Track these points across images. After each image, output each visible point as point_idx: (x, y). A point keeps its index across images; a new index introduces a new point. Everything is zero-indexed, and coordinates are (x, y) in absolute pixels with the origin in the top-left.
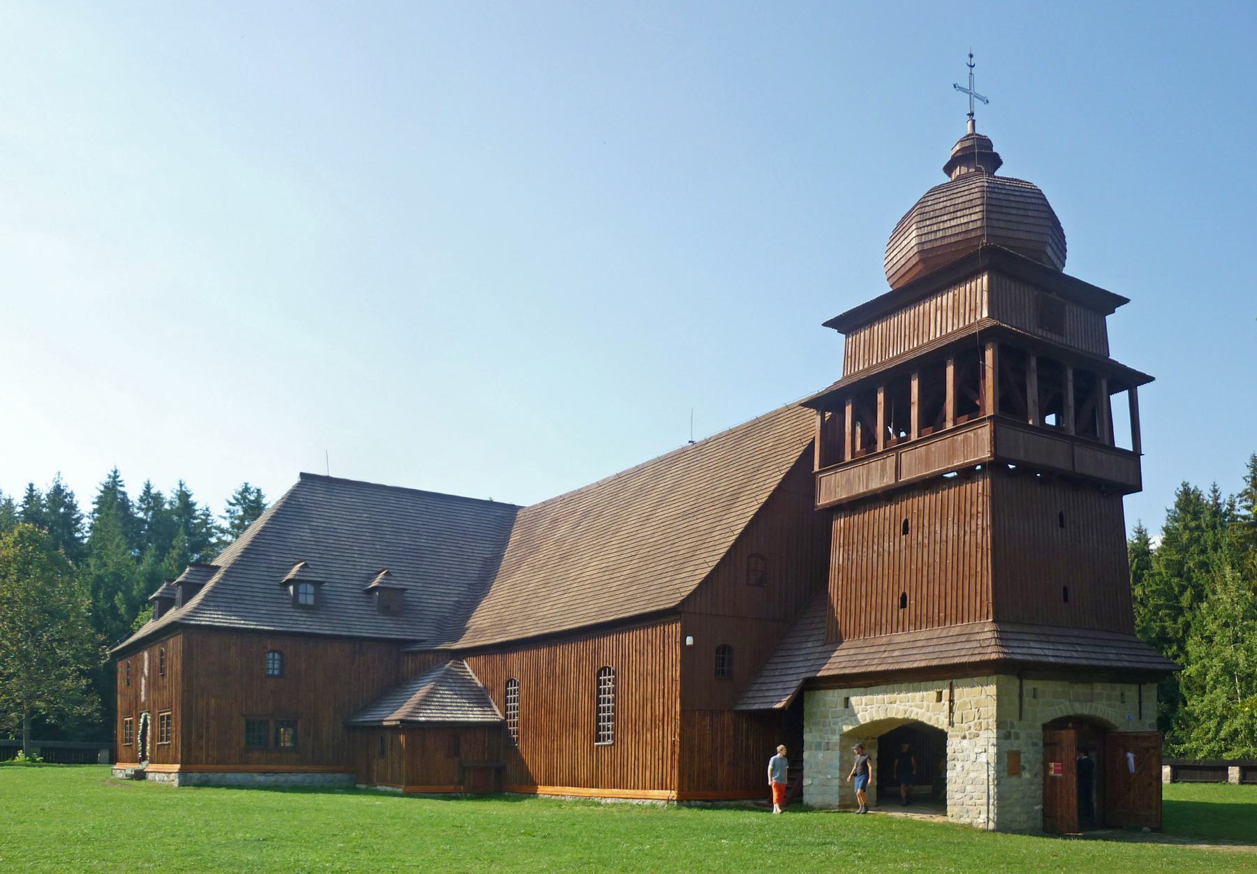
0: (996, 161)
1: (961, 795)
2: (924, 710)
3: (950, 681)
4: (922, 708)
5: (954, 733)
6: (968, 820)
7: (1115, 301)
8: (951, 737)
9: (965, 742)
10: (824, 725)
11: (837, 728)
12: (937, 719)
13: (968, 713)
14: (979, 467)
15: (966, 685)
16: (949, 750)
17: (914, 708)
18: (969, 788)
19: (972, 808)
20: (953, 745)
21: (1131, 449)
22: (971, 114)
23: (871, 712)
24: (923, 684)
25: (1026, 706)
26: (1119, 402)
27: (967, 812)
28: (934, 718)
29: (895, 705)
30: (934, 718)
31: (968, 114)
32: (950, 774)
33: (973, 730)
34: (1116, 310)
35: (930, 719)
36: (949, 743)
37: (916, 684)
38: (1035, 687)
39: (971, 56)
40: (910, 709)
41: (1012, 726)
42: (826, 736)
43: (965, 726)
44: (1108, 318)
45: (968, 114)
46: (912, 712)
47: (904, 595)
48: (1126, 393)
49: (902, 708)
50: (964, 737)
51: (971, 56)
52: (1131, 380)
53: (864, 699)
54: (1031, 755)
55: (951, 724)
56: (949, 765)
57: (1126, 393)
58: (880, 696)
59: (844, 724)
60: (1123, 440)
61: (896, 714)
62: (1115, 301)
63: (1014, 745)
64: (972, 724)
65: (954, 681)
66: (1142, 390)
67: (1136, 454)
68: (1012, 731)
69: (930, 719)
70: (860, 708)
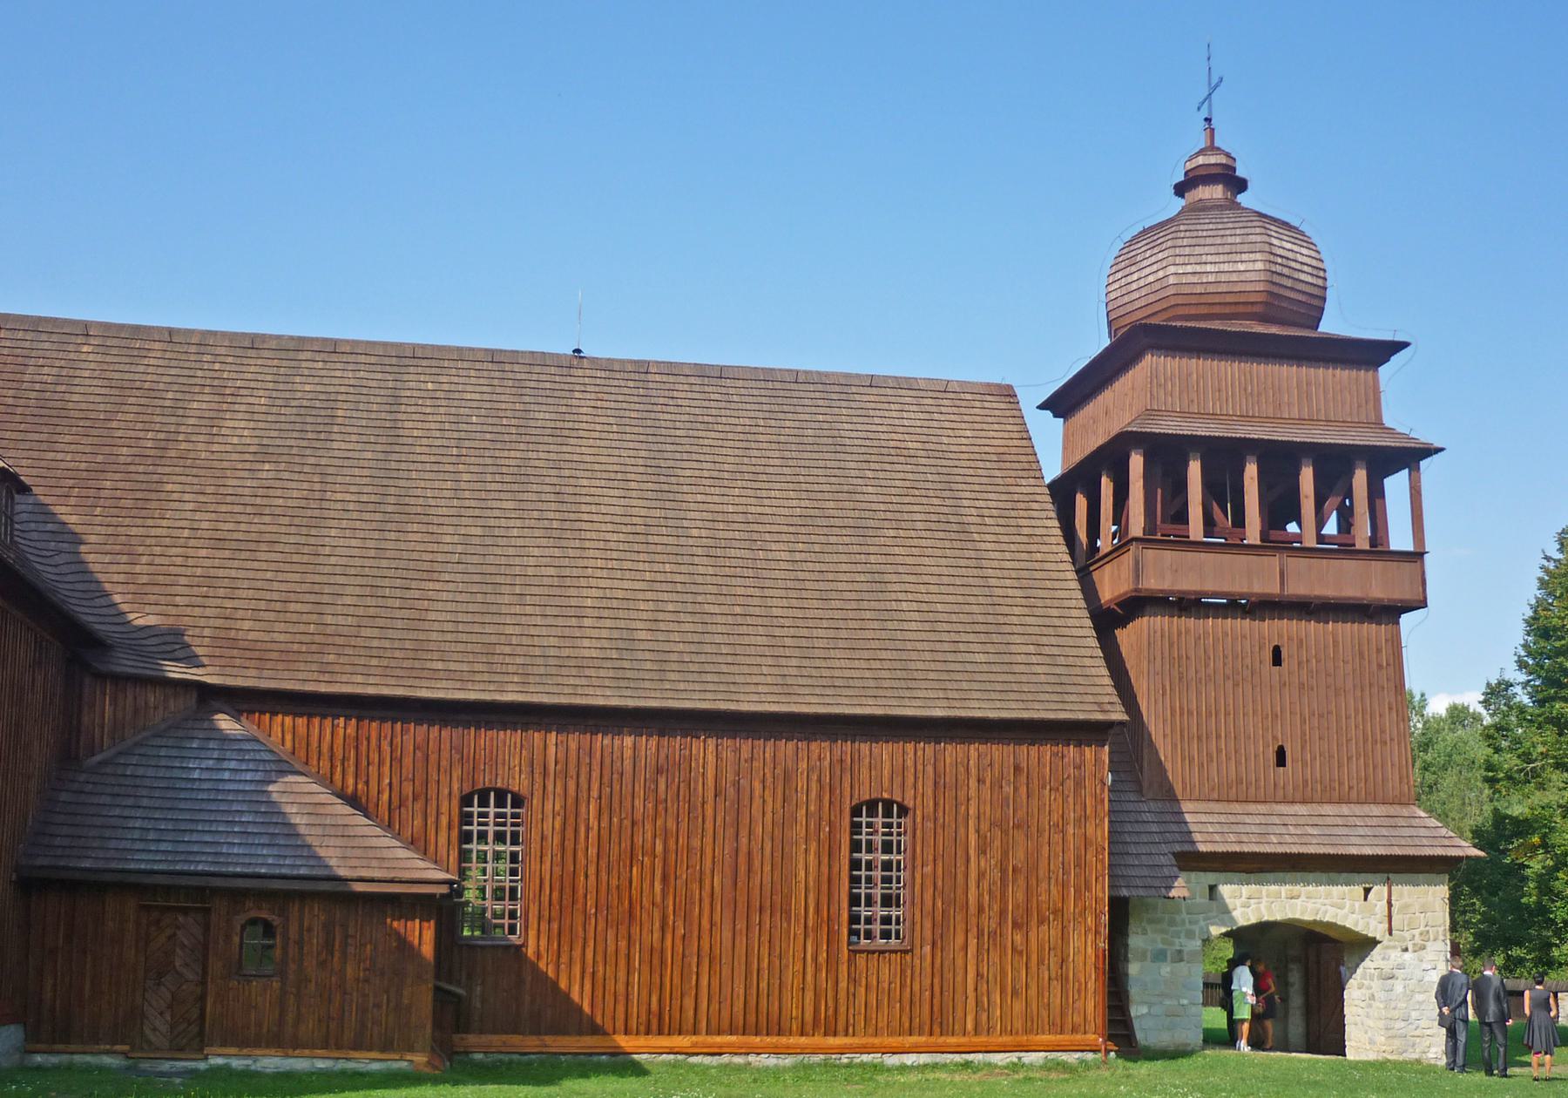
1: (1403, 1024)
2: (1346, 910)
4: (1341, 908)
5: (1392, 944)
6: (1415, 1056)
9: (1407, 956)
10: (1172, 923)
11: (1196, 928)
12: (1368, 924)
13: (1410, 918)
15: (1407, 883)
17: (1329, 907)
18: (1414, 1015)
19: (1418, 1040)
23: (1258, 909)
24: (1344, 875)
27: (1414, 1045)
28: (1361, 923)
29: (1298, 902)
30: (1361, 923)
31: (1206, 119)
35: (1356, 924)
37: (1333, 875)
40: (1323, 908)
42: (1177, 941)
43: (1407, 935)
45: (1206, 119)
46: (1326, 912)
49: (1310, 905)
50: (1406, 950)
53: (1246, 890)
58: (1273, 888)
59: (1212, 924)
61: (1302, 914)
64: (1416, 932)
70: (1238, 902)
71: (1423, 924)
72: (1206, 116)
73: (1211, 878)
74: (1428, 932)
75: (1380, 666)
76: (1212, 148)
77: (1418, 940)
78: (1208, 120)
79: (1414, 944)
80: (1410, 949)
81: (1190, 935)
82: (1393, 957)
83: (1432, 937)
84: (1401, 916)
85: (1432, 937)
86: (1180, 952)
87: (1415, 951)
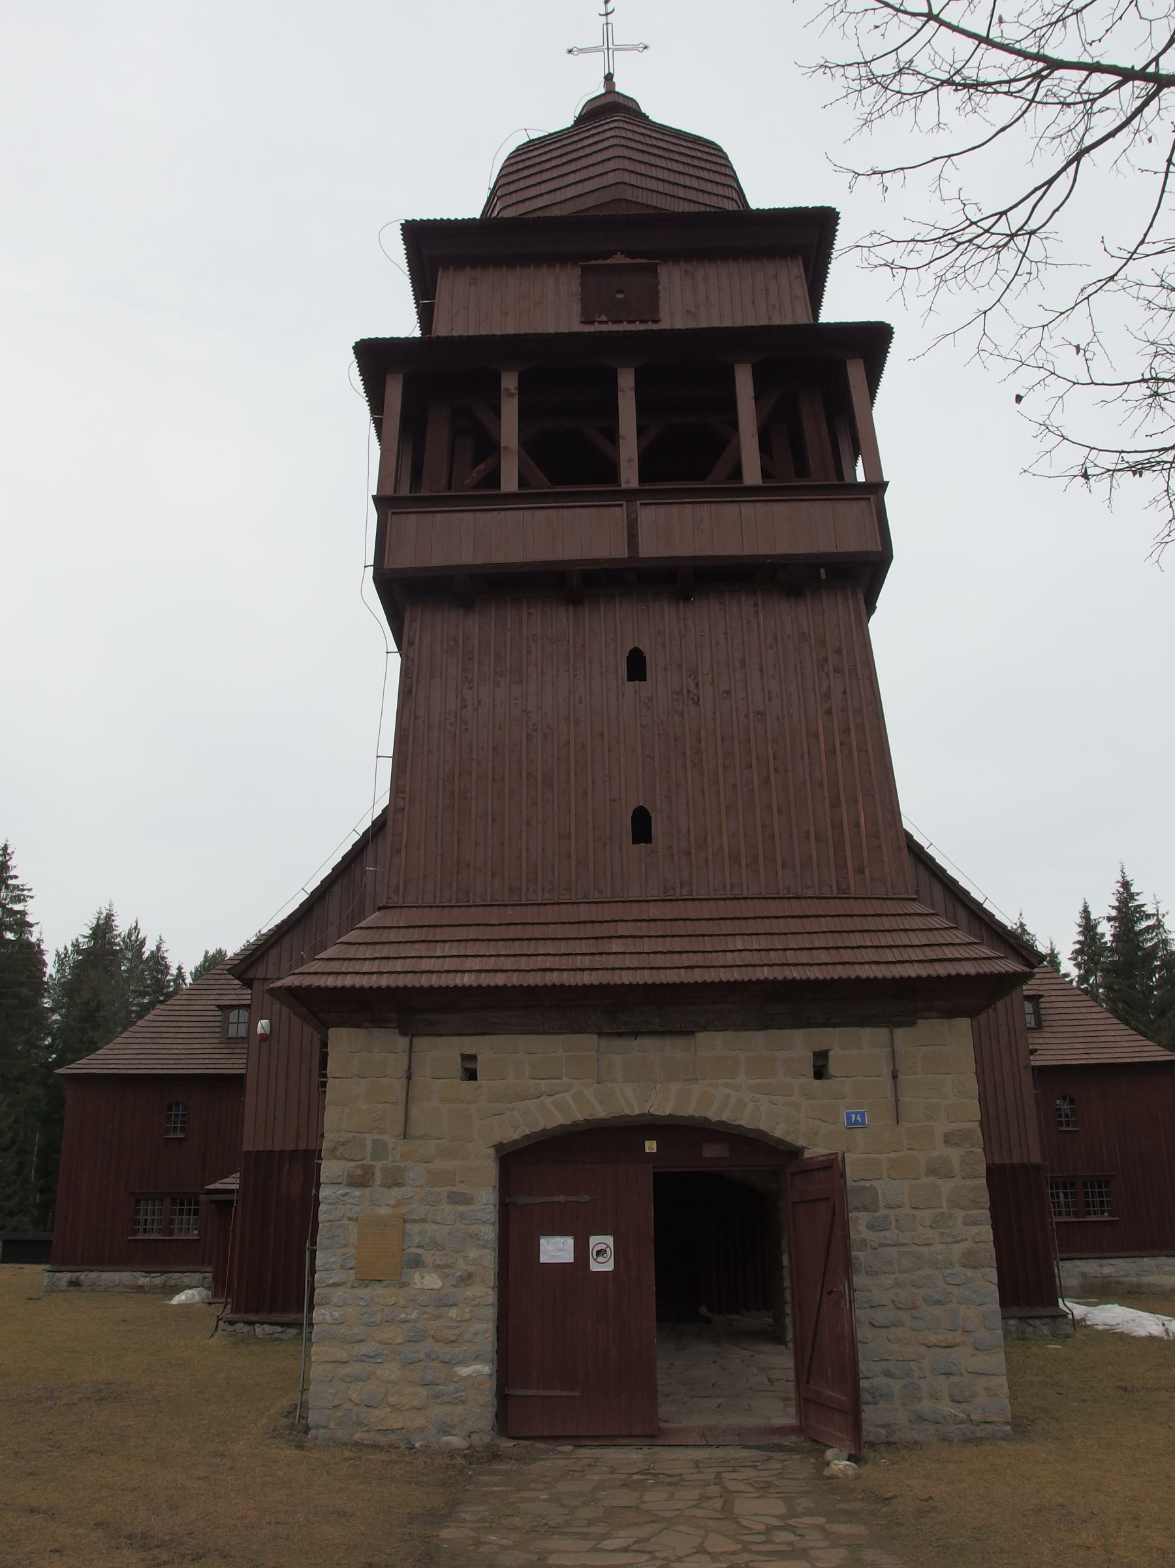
38: (468, 1051)
68: (378, 1165)
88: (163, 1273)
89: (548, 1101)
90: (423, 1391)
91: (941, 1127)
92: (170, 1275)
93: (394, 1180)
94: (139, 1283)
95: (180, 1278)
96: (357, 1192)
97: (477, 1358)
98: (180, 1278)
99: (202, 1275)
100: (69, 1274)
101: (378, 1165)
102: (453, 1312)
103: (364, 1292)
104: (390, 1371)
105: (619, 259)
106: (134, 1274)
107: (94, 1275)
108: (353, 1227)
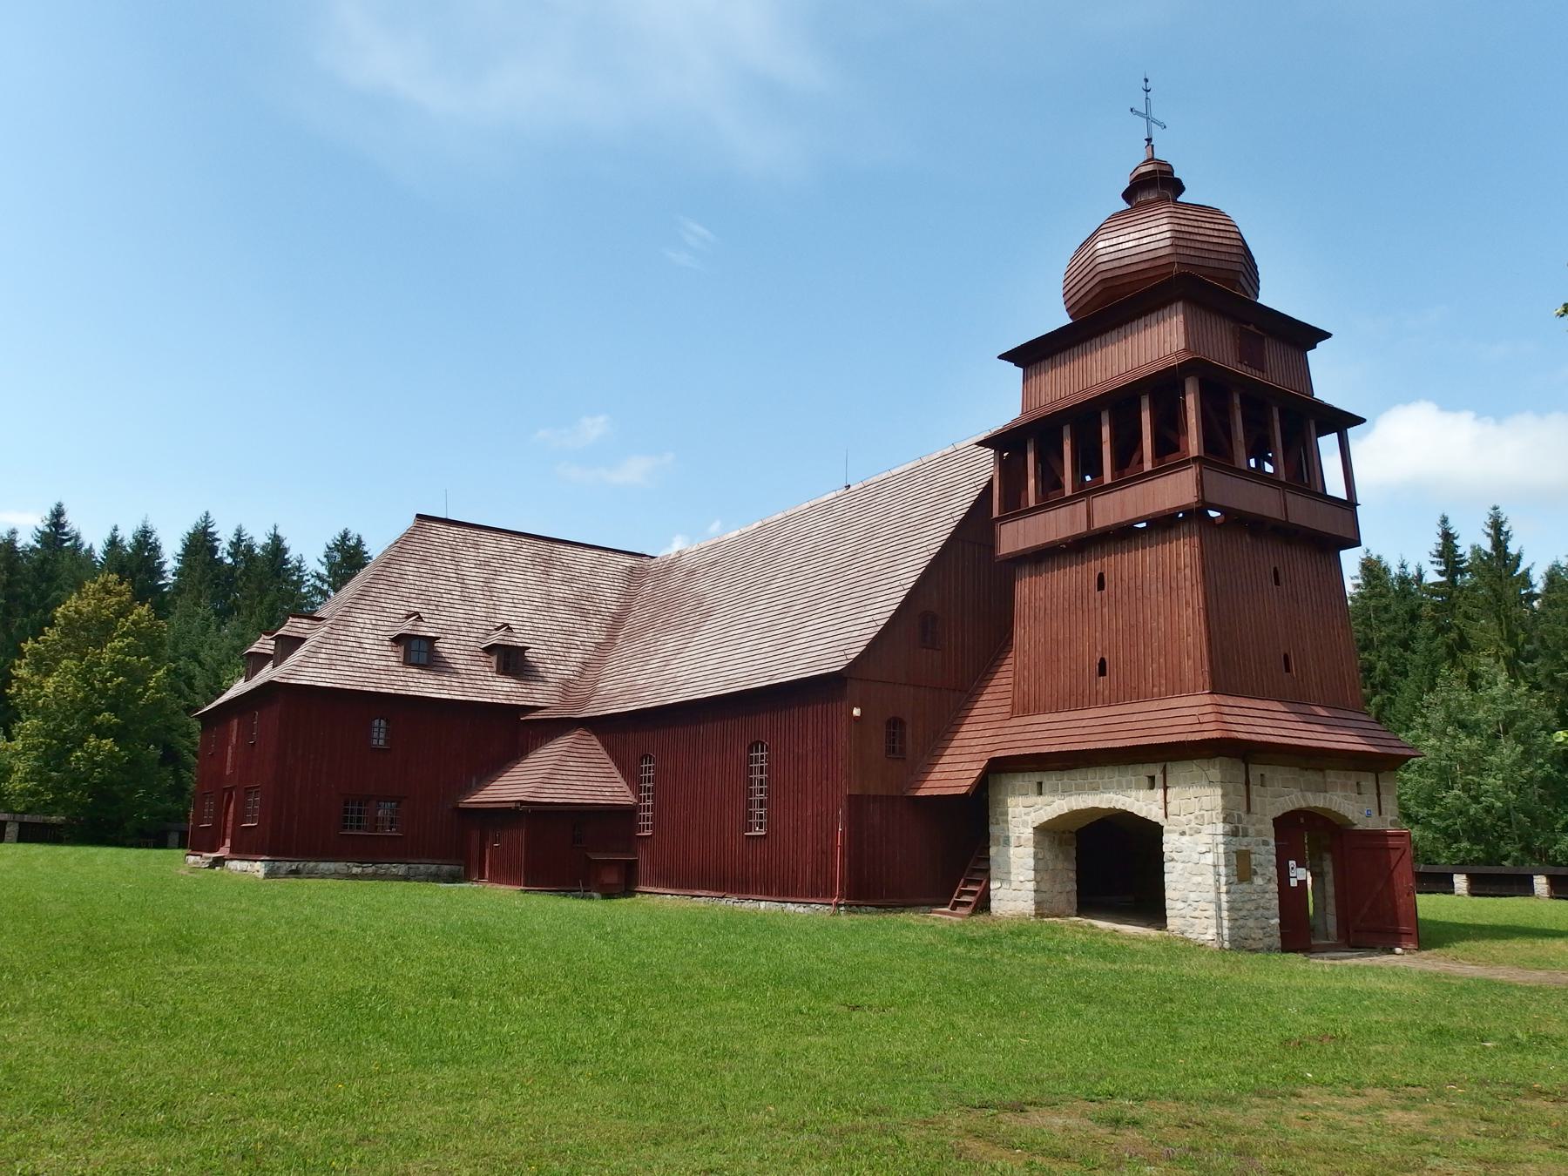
0: (1178, 187)
1: (1181, 905)
2: (1133, 799)
3: (1163, 764)
7: (1315, 336)
8: (1170, 832)
9: (1185, 839)
12: (1151, 810)
13: (1186, 803)
14: (1181, 515)
16: (1165, 848)
19: (1197, 921)
20: (1170, 842)
21: (1343, 495)
22: (1149, 140)
25: (1253, 796)
26: (1328, 445)
28: (1145, 808)
31: (1146, 140)
32: (1167, 878)
33: (1193, 824)
34: (1318, 344)
36: (1165, 838)
39: (1146, 80)
41: (1240, 821)
44: (1309, 353)
45: (1146, 140)
47: (1103, 660)
48: (1335, 435)
50: (1183, 833)
51: (1146, 80)
52: (1341, 422)
54: (1265, 856)
55: (1166, 816)
56: (1167, 867)
57: (1335, 435)
60: (1335, 486)
62: (1315, 336)
63: (1242, 843)
65: (1168, 764)
66: (1351, 431)
67: (1350, 504)
69: (1141, 809)
71: (1197, 809)
72: (1147, 137)
73: (1037, 777)
74: (1202, 816)
75: (1178, 569)
76: (1150, 160)
77: (1193, 824)
78: (1149, 140)
79: (1190, 828)
80: (1187, 833)
81: (1025, 824)
82: (1172, 841)
83: (1206, 822)
84: (1177, 802)
85: (1206, 822)
86: (1018, 837)
87: (1192, 835)
88: (374, 864)
89: (1287, 797)
90: (1260, 931)
91: (1390, 818)
92: (380, 865)
93: (1246, 835)
94: (353, 872)
95: (389, 868)
96: (1234, 839)
97: (1276, 917)
98: (389, 868)
99: (407, 866)
100: (288, 864)
101: (1240, 825)
102: (1267, 896)
103: (1240, 887)
104: (1251, 923)
105: (1252, 328)
106: (348, 864)
107: (312, 864)
108: (1234, 856)
